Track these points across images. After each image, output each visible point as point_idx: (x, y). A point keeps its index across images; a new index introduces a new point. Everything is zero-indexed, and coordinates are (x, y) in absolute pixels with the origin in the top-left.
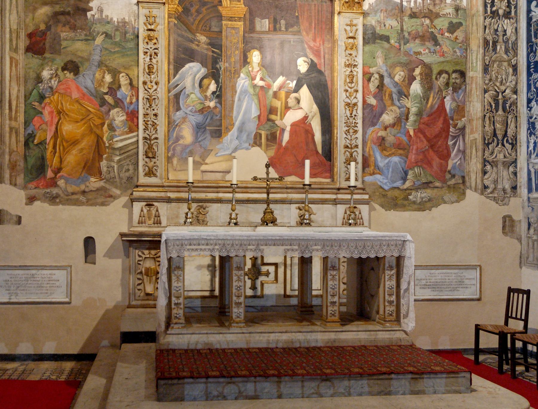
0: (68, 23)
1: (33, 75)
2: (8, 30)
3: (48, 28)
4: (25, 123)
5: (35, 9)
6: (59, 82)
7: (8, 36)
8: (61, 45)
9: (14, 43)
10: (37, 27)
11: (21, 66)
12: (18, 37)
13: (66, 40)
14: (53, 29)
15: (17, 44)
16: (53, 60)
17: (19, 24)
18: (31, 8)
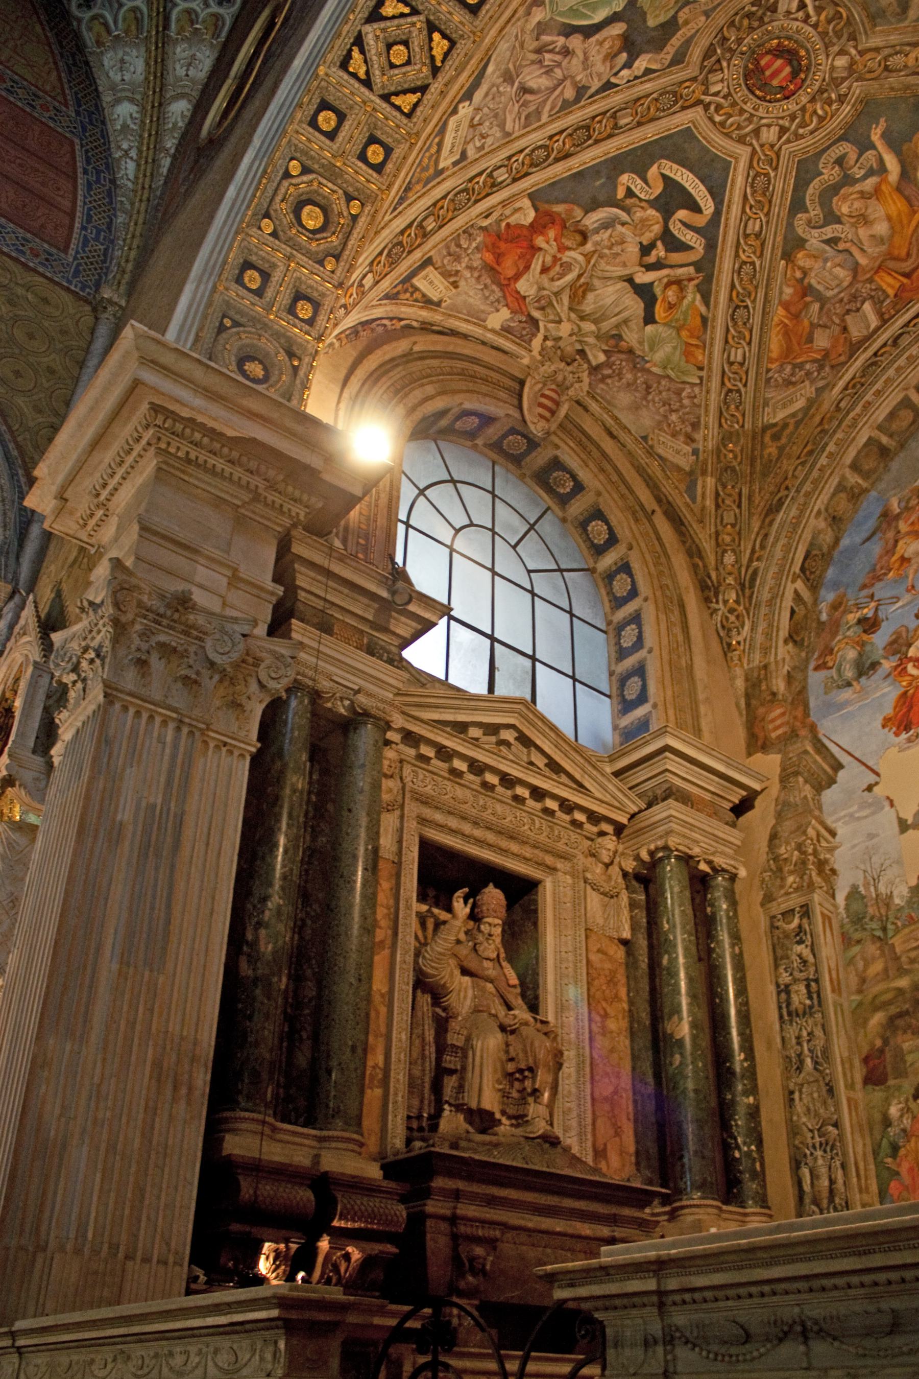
0: (909, 1026)
1: (877, 1116)
2: (839, 1060)
3: (886, 1042)
4: (880, 1193)
5: (866, 1021)
6: (914, 1117)
7: (840, 1069)
8: (905, 1062)
9: (849, 1075)
10: (872, 1044)
11: (861, 1107)
12: (852, 1066)
13: (910, 1052)
14: (892, 1043)
15: (852, 1078)
16: (899, 1088)
17: (850, 1049)
18: (861, 1021)
